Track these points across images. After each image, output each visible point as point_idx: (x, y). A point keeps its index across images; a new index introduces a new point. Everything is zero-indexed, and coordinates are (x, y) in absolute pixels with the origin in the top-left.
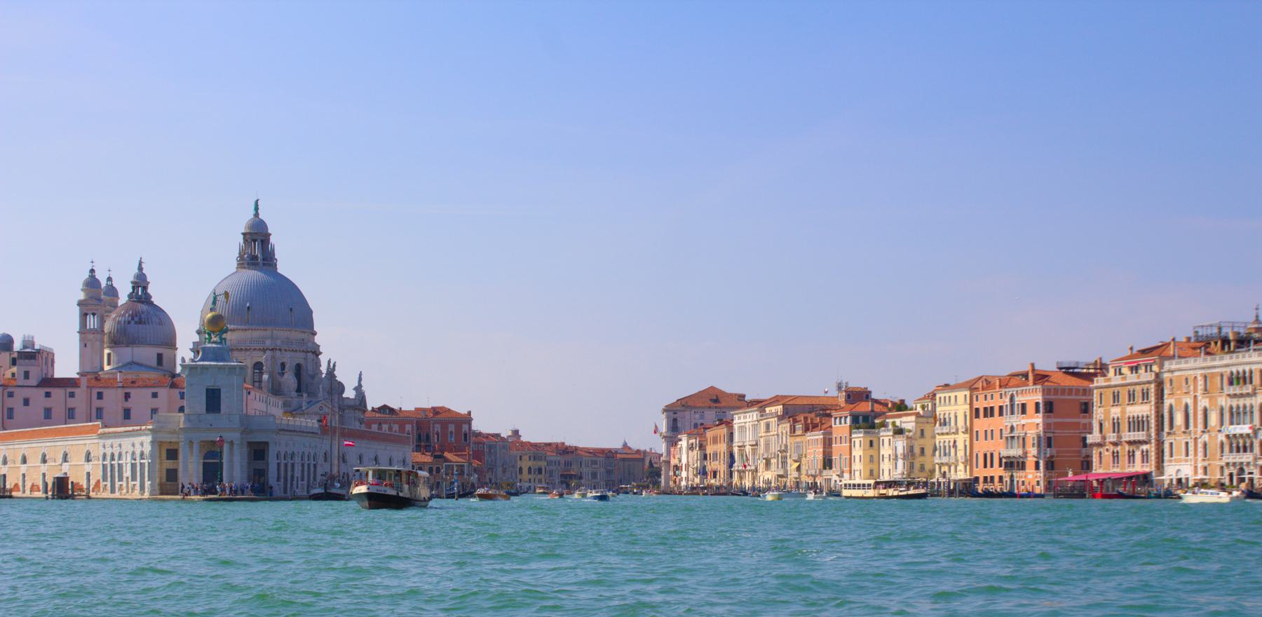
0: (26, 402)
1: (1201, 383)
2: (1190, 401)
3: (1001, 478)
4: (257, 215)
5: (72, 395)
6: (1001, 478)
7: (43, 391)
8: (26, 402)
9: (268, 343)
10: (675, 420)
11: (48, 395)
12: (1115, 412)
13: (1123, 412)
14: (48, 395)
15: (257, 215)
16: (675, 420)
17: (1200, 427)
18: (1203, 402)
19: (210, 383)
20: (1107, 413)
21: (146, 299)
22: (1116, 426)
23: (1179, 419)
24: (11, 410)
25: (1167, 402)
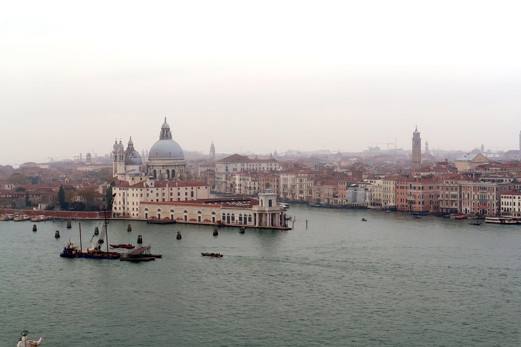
0: (152, 192)
1: (472, 188)
2: (470, 193)
3: (407, 206)
4: (165, 122)
5: (164, 189)
6: (407, 206)
7: (156, 189)
8: (152, 192)
9: (177, 164)
10: (227, 167)
11: (157, 189)
12: (447, 192)
13: (449, 193)
14: (157, 189)
15: (165, 122)
16: (227, 167)
17: (472, 199)
18: (473, 193)
19: (269, 199)
20: (444, 193)
21: (133, 149)
22: (447, 196)
23: (466, 196)
24: (148, 194)
25: (463, 192)
